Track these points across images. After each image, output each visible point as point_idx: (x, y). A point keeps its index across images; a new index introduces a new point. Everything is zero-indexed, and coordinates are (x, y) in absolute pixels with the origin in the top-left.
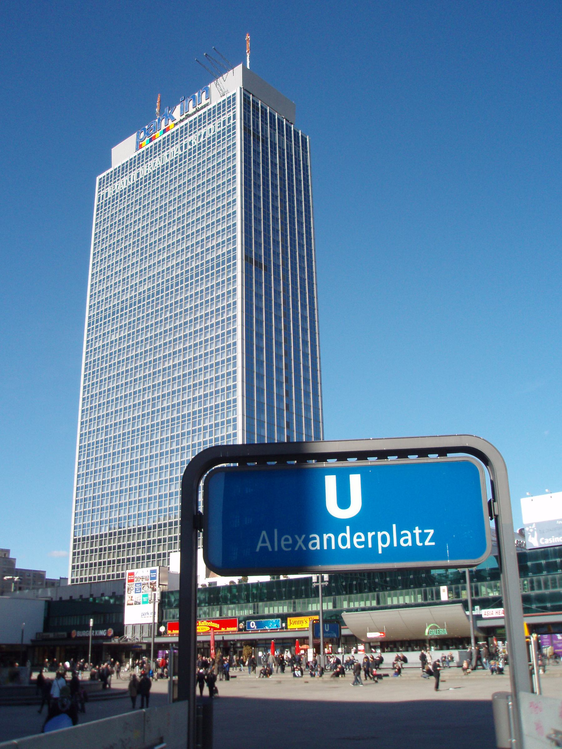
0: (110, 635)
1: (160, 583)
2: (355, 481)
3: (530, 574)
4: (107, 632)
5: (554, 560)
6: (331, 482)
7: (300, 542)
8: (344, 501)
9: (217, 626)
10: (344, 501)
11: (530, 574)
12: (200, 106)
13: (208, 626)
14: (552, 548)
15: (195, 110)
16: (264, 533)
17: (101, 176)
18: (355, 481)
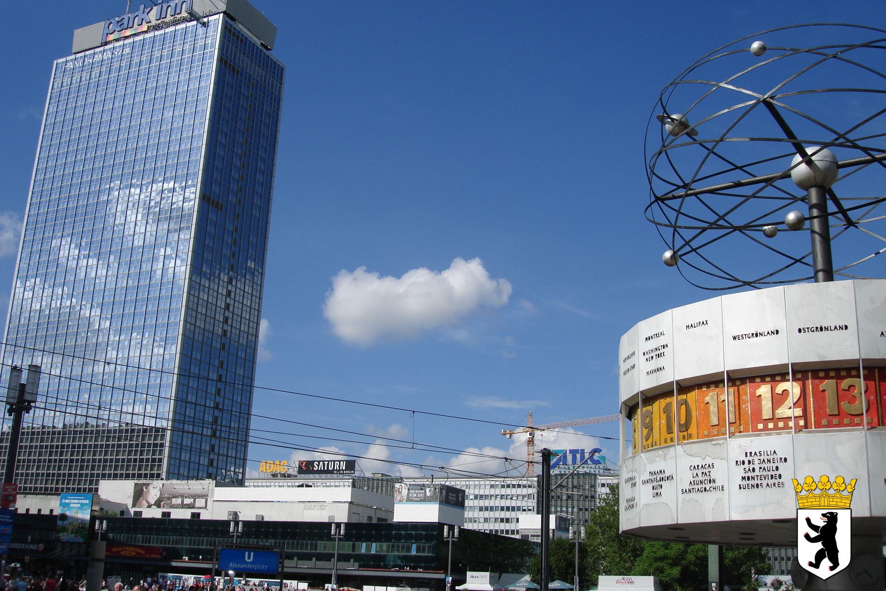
0: (40, 549)
1: (93, 509)
2: (252, 554)
3: (393, 540)
4: (37, 546)
5: (411, 532)
6: (247, 553)
7: (239, 566)
8: (249, 558)
9: (142, 552)
10: (249, 558)
11: (393, 540)
12: (178, 16)
13: (134, 551)
14: (411, 523)
15: (172, 18)
16: (231, 563)
17: (60, 61)
18: (252, 554)
